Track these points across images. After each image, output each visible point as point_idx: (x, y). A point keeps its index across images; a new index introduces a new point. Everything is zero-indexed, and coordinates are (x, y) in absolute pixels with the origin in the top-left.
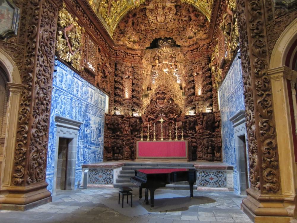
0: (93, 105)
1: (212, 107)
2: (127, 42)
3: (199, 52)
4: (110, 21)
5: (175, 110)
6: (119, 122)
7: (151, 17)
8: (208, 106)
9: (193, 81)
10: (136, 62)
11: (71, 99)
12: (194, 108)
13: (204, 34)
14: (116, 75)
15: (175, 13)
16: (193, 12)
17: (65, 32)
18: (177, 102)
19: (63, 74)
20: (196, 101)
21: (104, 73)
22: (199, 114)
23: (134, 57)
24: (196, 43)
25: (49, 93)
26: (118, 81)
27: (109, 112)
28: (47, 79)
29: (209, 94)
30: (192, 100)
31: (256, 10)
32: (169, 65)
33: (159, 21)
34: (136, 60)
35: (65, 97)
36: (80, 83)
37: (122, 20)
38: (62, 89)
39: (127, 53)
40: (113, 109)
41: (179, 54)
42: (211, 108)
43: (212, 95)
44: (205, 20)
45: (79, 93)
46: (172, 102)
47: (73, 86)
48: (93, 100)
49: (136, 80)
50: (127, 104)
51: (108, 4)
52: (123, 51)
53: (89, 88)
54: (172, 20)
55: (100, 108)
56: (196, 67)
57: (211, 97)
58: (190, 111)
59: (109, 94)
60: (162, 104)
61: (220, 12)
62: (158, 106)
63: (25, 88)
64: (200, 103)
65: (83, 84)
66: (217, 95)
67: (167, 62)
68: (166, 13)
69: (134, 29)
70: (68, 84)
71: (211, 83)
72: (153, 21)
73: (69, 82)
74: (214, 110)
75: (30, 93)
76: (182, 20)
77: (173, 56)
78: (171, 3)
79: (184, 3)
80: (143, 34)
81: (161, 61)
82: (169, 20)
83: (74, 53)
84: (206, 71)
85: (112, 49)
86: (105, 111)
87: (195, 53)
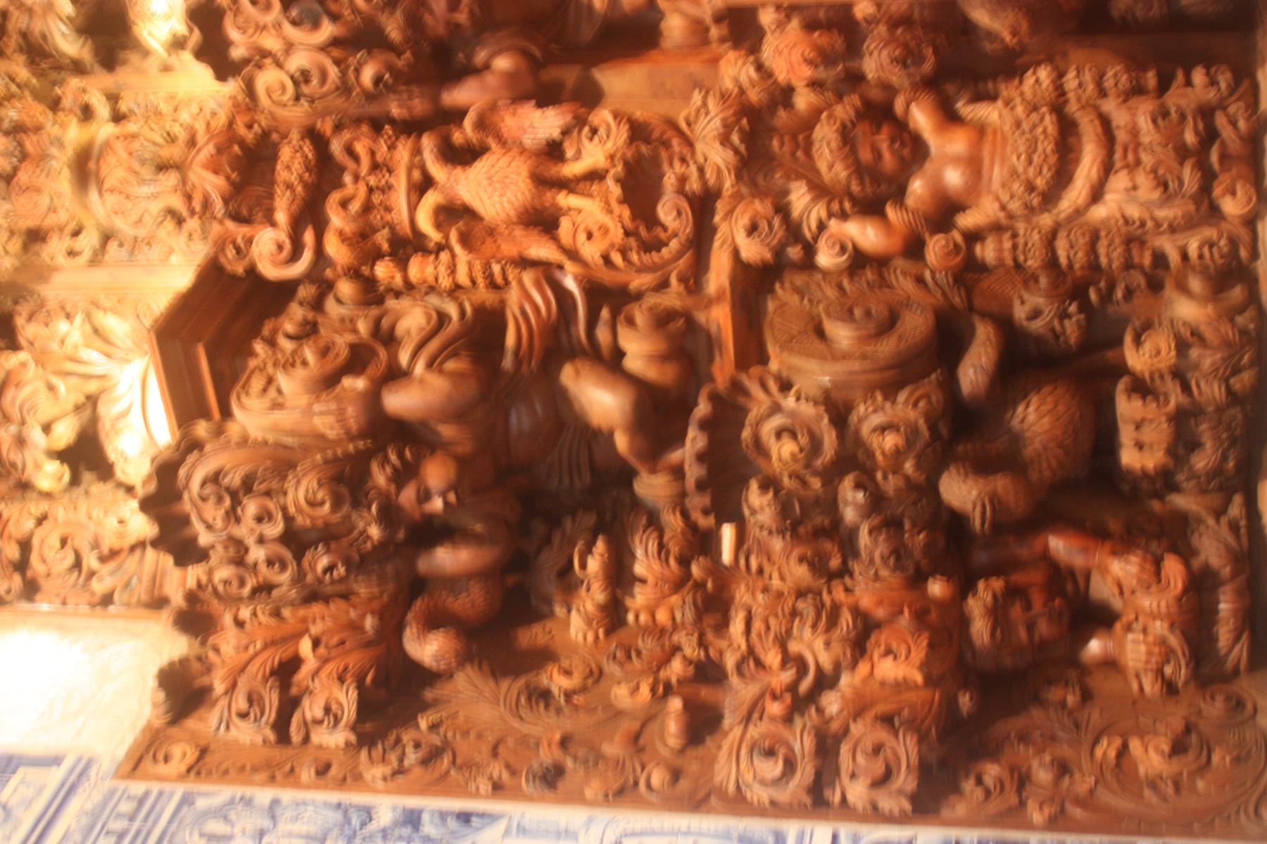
6: (325, 421)
86: (84, 769)
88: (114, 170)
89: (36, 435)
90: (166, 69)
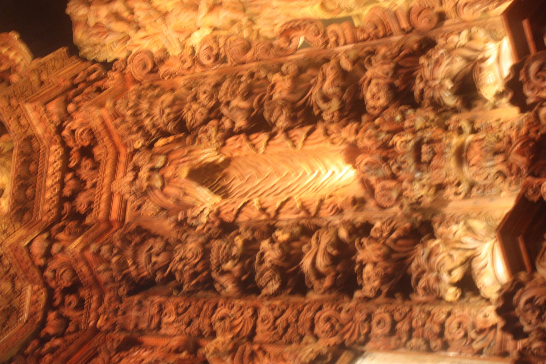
10: (112, 127)
39: (62, 199)
52: (38, 248)
88: (474, 156)
89: (445, 277)
90: (495, 107)
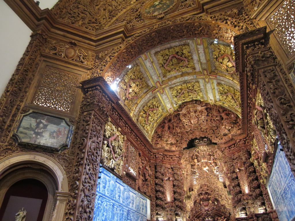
0: (134, 210)
1: (265, 206)
2: (164, 145)
3: (237, 147)
4: (148, 128)
5: (222, 213)
7: (185, 121)
8: (259, 206)
9: (237, 178)
10: (174, 163)
11: (113, 206)
12: (244, 209)
13: (238, 130)
14: (156, 178)
15: (206, 114)
16: (223, 112)
17: (110, 141)
18: (223, 202)
19: (106, 180)
20: (244, 200)
21: (145, 177)
22: (252, 215)
23: (173, 158)
24: (232, 139)
25: (92, 200)
26: (159, 183)
27: (151, 218)
28: (92, 186)
29: (257, 191)
30: (240, 199)
31: (285, 104)
32: (208, 163)
33: (193, 123)
34: (175, 161)
35: (107, 204)
36: (122, 188)
37: (159, 126)
38: (104, 195)
39: (166, 155)
40: (155, 214)
41: (216, 151)
42: (264, 207)
43: (262, 192)
44: (236, 117)
45: (121, 198)
46: (217, 202)
47: (115, 192)
48: (134, 206)
49: (176, 181)
50: (170, 208)
51: (146, 114)
52: (161, 154)
53: (130, 192)
54: (205, 121)
55: (142, 214)
56: (237, 162)
57: (261, 194)
58: (240, 213)
59: (150, 197)
60: (207, 206)
61: (249, 109)
62: (202, 209)
63: (71, 196)
64: (250, 202)
65: (124, 188)
66: (267, 191)
67: (206, 161)
68: (198, 115)
69: (171, 133)
70: (111, 190)
71: (257, 179)
72: (187, 123)
73: (111, 188)
74: (268, 209)
75: (75, 201)
76: (214, 120)
77: (210, 153)
78: (202, 106)
79: (214, 106)
80: (179, 136)
81: (200, 160)
82: (202, 121)
83: (117, 160)
84: (249, 166)
85: (151, 152)
86: (146, 217)
87: (233, 148)
